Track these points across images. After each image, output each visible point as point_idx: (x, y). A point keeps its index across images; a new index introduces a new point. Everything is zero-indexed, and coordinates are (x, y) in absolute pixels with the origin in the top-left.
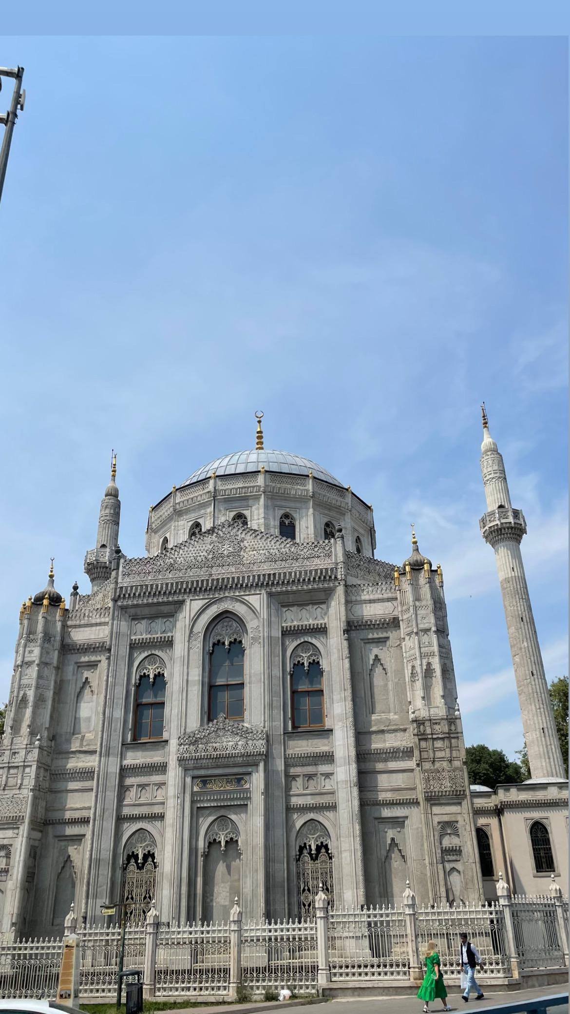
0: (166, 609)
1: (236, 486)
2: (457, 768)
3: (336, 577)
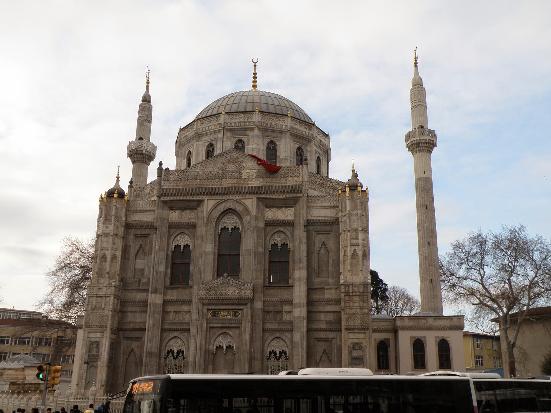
0: (192, 204)
1: (239, 121)
2: (365, 313)
3: (301, 191)
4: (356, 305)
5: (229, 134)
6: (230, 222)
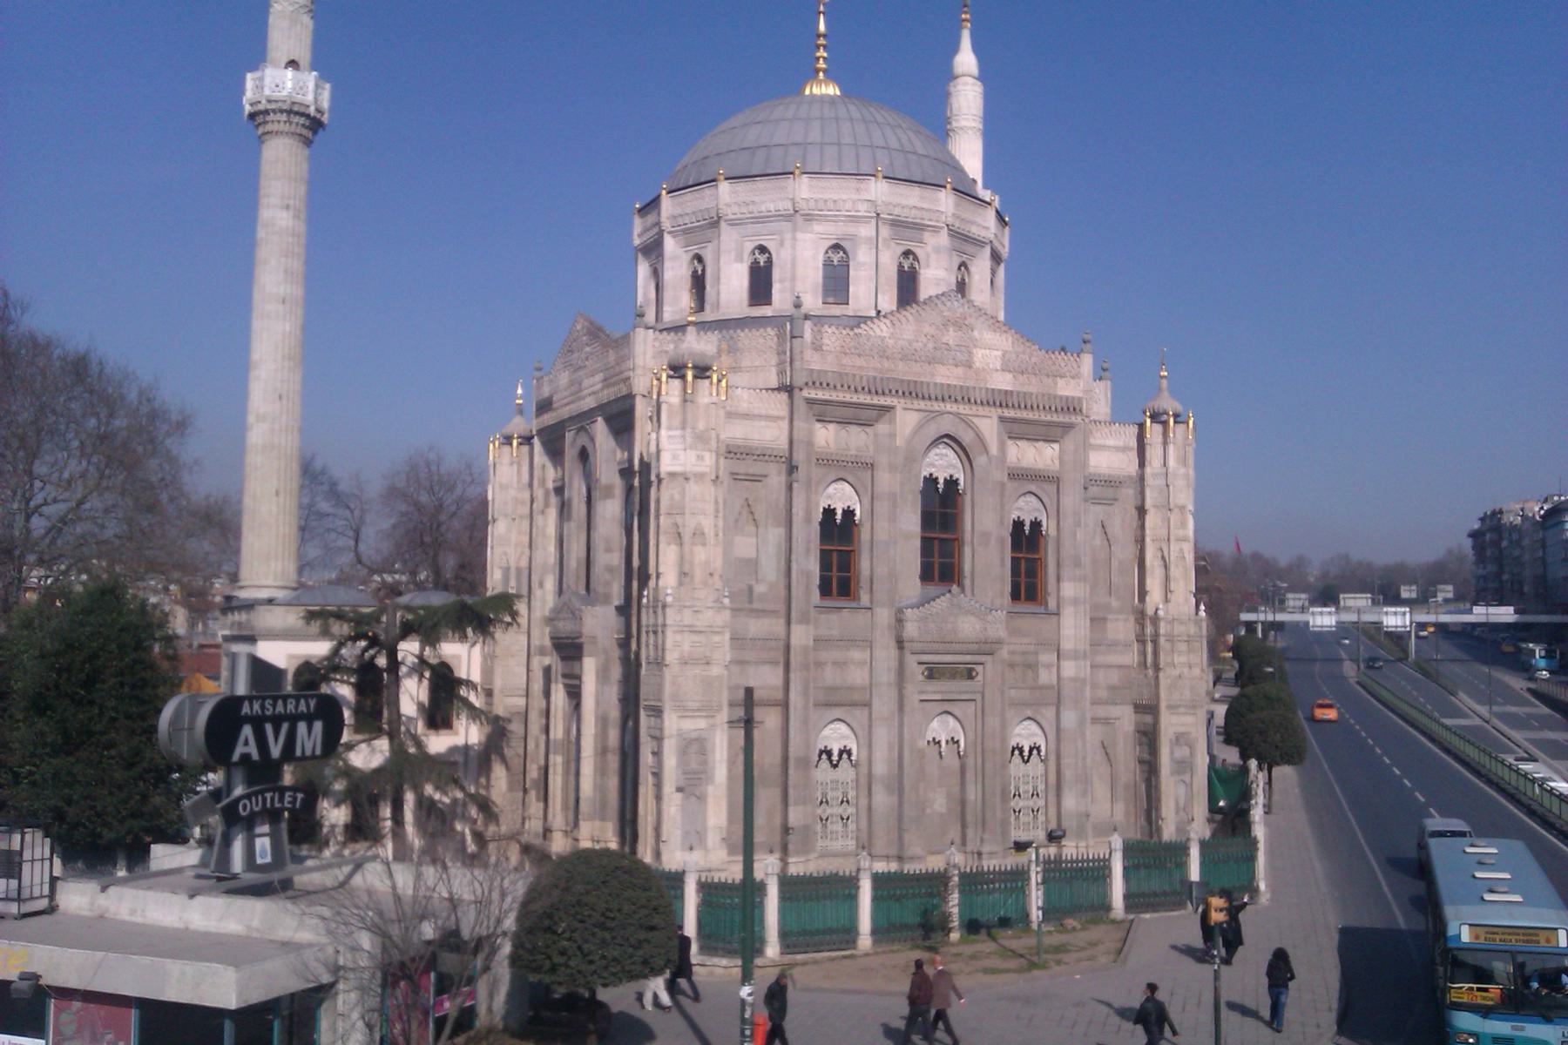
4: (1183, 659)
5: (885, 232)
6: (943, 464)
